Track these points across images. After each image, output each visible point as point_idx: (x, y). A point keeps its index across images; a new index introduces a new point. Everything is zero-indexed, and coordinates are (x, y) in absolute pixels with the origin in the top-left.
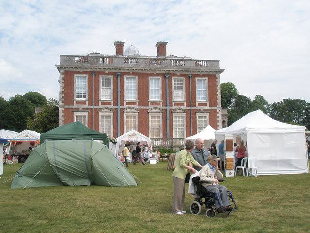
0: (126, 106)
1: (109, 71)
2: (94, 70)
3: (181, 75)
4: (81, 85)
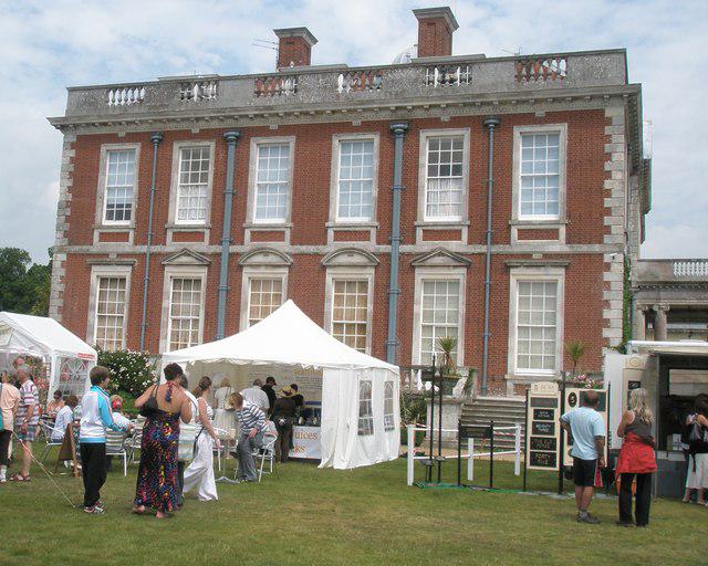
0: (249, 244)
2: (159, 127)
3: (456, 122)
4: (119, 178)
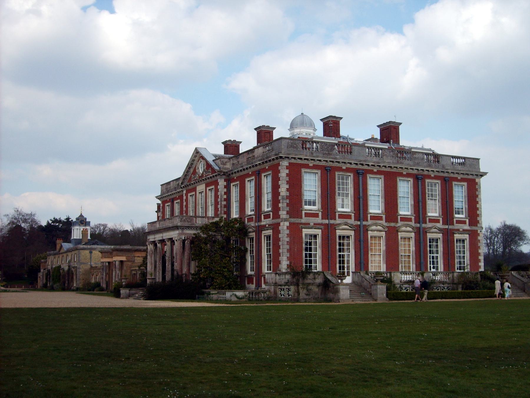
1: (349, 166)
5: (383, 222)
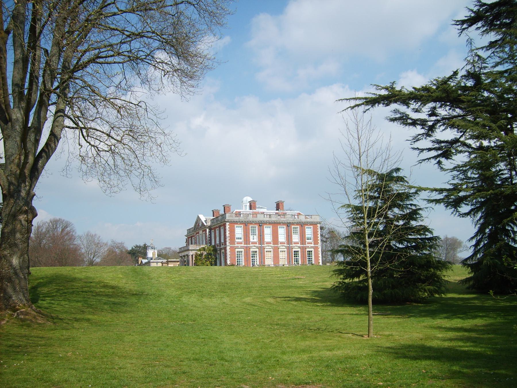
5: (272, 245)
